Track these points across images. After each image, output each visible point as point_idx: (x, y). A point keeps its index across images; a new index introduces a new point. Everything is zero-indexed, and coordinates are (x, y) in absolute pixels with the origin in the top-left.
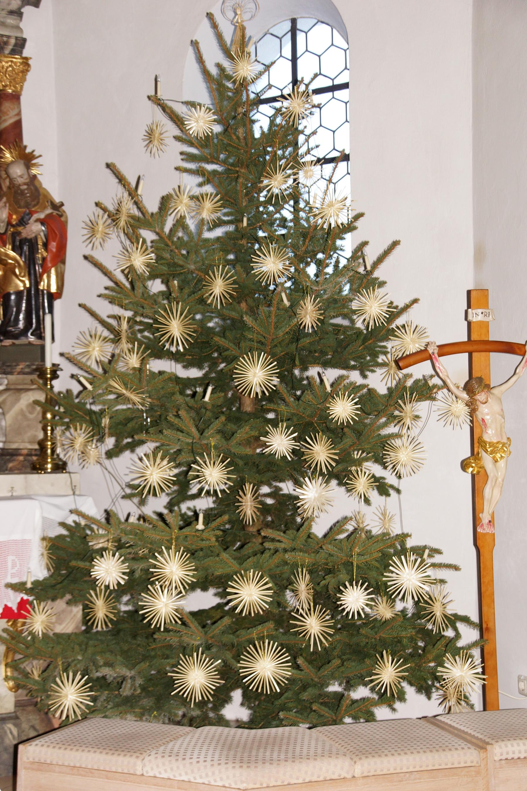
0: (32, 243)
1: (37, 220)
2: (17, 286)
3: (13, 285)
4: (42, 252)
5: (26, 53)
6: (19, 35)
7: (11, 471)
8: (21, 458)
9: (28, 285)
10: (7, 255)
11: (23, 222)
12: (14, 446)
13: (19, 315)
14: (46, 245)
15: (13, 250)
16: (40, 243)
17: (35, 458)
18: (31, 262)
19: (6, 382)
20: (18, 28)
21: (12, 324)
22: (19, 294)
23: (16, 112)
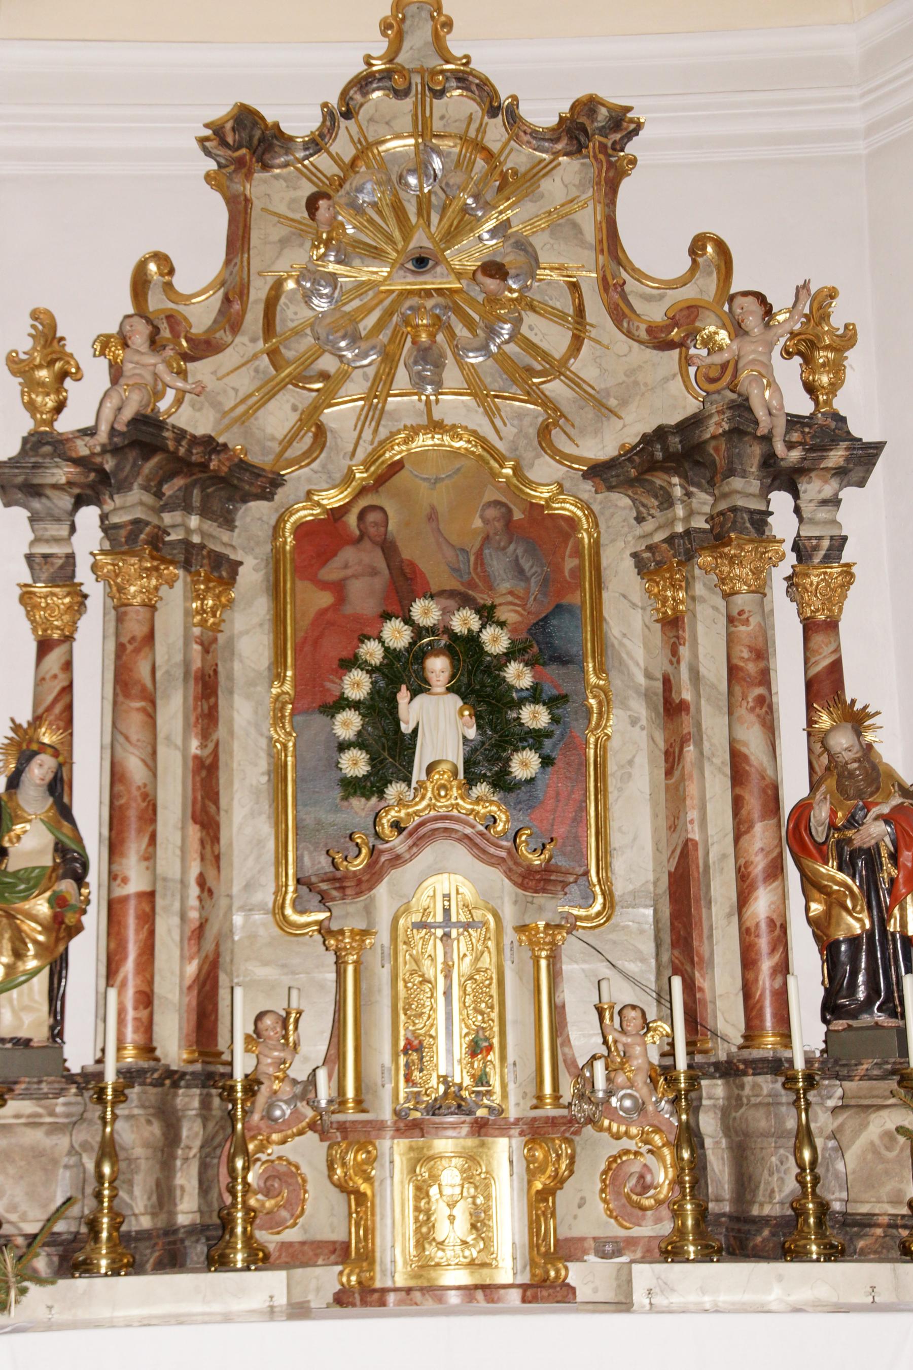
0: (871, 856)
1: (877, 818)
2: (849, 928)
3: (843, 926)
4: (888, 870)
5: (847, 556)
6: (835, 532)
7: (862, 1256)
8: (879, 1231)
9: (868, 926)
10: (833, 879)
11: (853, 822)
12: (864, 1209)
13: (856, 978)
14: (894, 858)
15: (840, 869)
16: (884, 853)
17: (904, 1233)
18: (871, 886)
19: (839, 1092)
20: (835, 522)
21: (844, 993)
22: (854, 941)
23: (832, 647)
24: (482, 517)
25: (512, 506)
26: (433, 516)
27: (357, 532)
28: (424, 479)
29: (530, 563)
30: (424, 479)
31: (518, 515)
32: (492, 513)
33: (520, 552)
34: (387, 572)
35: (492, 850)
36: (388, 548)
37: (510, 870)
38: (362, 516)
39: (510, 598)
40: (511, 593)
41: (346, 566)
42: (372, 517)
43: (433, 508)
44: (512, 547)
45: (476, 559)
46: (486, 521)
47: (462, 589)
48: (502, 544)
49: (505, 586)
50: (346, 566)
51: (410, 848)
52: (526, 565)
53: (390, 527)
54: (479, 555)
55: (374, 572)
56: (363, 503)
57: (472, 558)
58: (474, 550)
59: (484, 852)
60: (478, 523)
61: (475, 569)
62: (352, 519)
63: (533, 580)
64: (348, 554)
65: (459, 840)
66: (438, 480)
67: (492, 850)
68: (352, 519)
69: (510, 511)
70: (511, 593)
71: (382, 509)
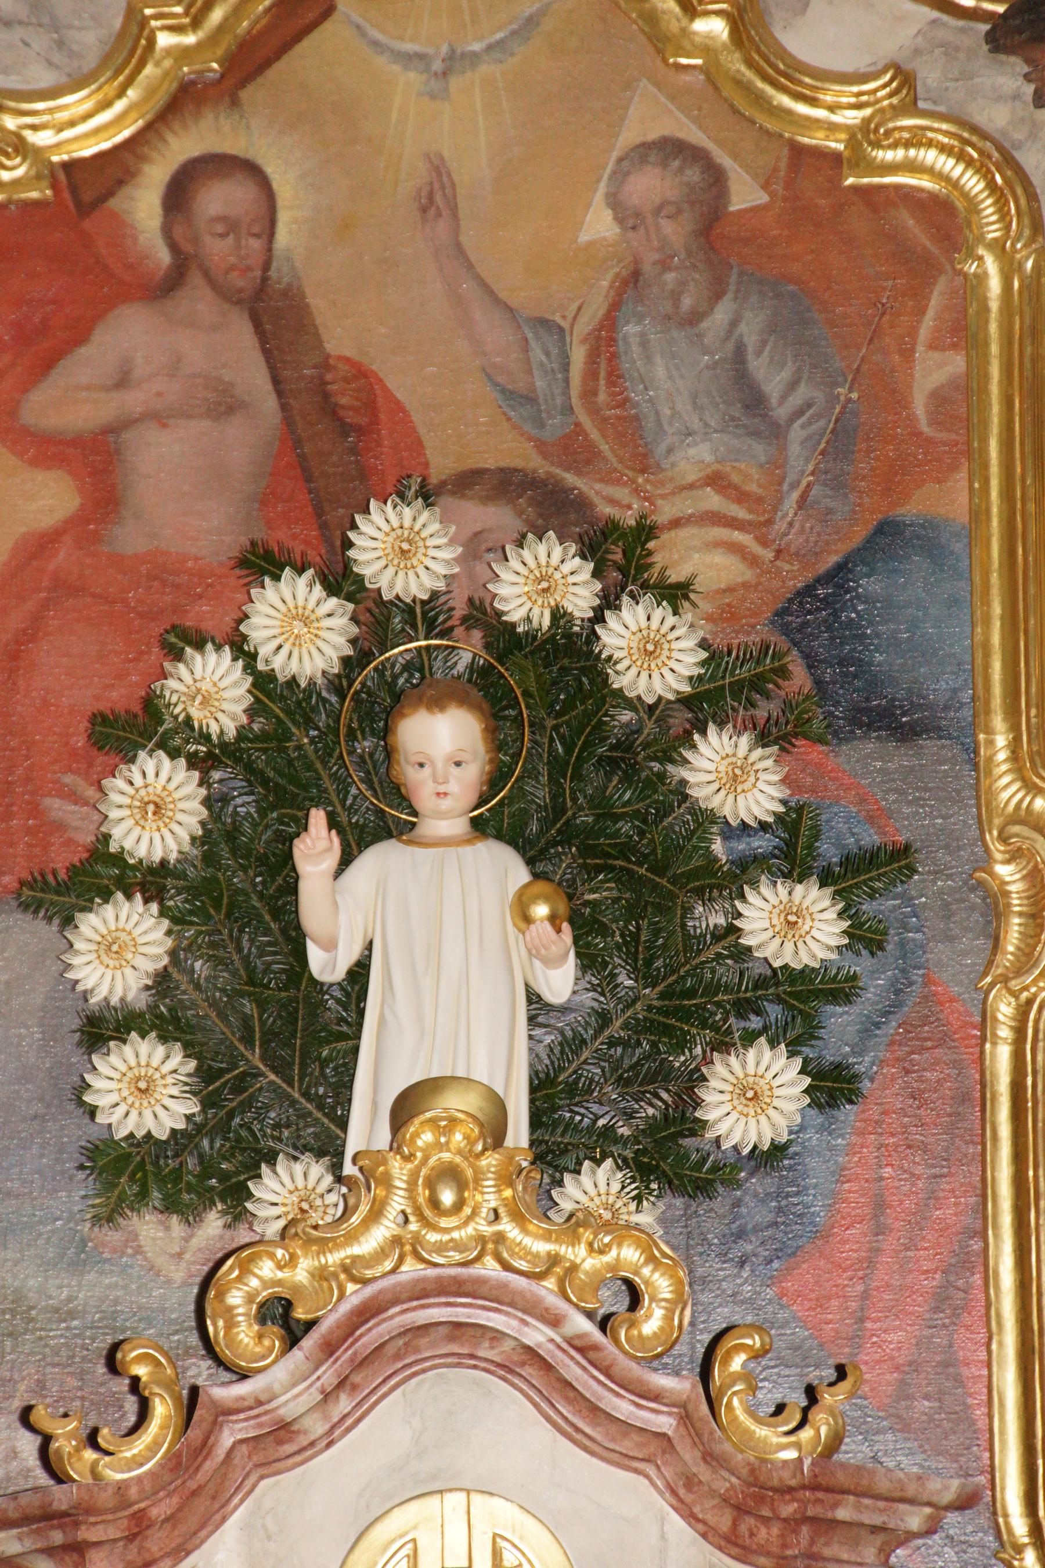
24: (614, 202)
25: (724, 160)
26: (436, 199)
27: (164, 256)
28: (408, 59)
29: (786, 374)
30: (408, 59)
31: (745, 194)
32: (649, 185)
33: (750, 331)
34: (270, 403)
35: (623, 1407)
36: (275, 314)
37: (691, 1482)
38: (178, 194)
39: (712, 500)
40: (716, 480)
41: (123, 381)
42: (217, 199)
43: (438, 168)
44: (721, 314)
45: (593, 357)
46: (628, 217)
47: (538, 464)
48: (687, 302)
49: (694, 457)
50: (123, 381)
51: (328, 1396)
52: (772, 377)
53: (283, 238)
54: (605, 340)
55: (225, 405)
56: (183, 145)
57: (578, 355)
58: (584, 325)
59: (594, 1412)
60: (599, 225)
61: (589, 394)
62: (144, 205)
63: (797, 433)
64: (129, 335)
65: (505, 1370)
66: (456, 62)
67: (623, 1407)
68: (144, 205)
69: (717, 177)
70: (716, 480)
71: (253, 170)
